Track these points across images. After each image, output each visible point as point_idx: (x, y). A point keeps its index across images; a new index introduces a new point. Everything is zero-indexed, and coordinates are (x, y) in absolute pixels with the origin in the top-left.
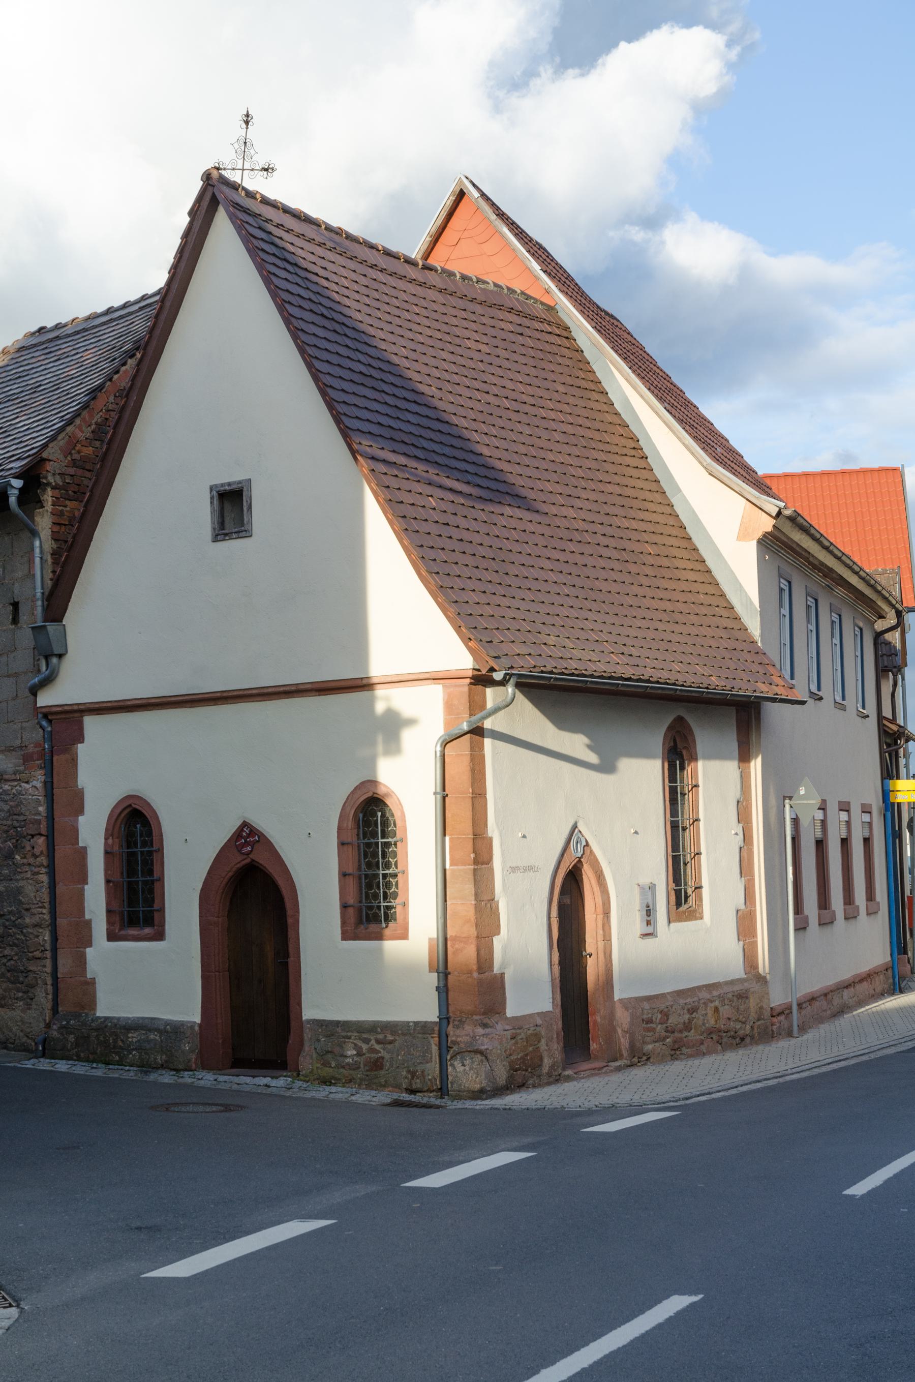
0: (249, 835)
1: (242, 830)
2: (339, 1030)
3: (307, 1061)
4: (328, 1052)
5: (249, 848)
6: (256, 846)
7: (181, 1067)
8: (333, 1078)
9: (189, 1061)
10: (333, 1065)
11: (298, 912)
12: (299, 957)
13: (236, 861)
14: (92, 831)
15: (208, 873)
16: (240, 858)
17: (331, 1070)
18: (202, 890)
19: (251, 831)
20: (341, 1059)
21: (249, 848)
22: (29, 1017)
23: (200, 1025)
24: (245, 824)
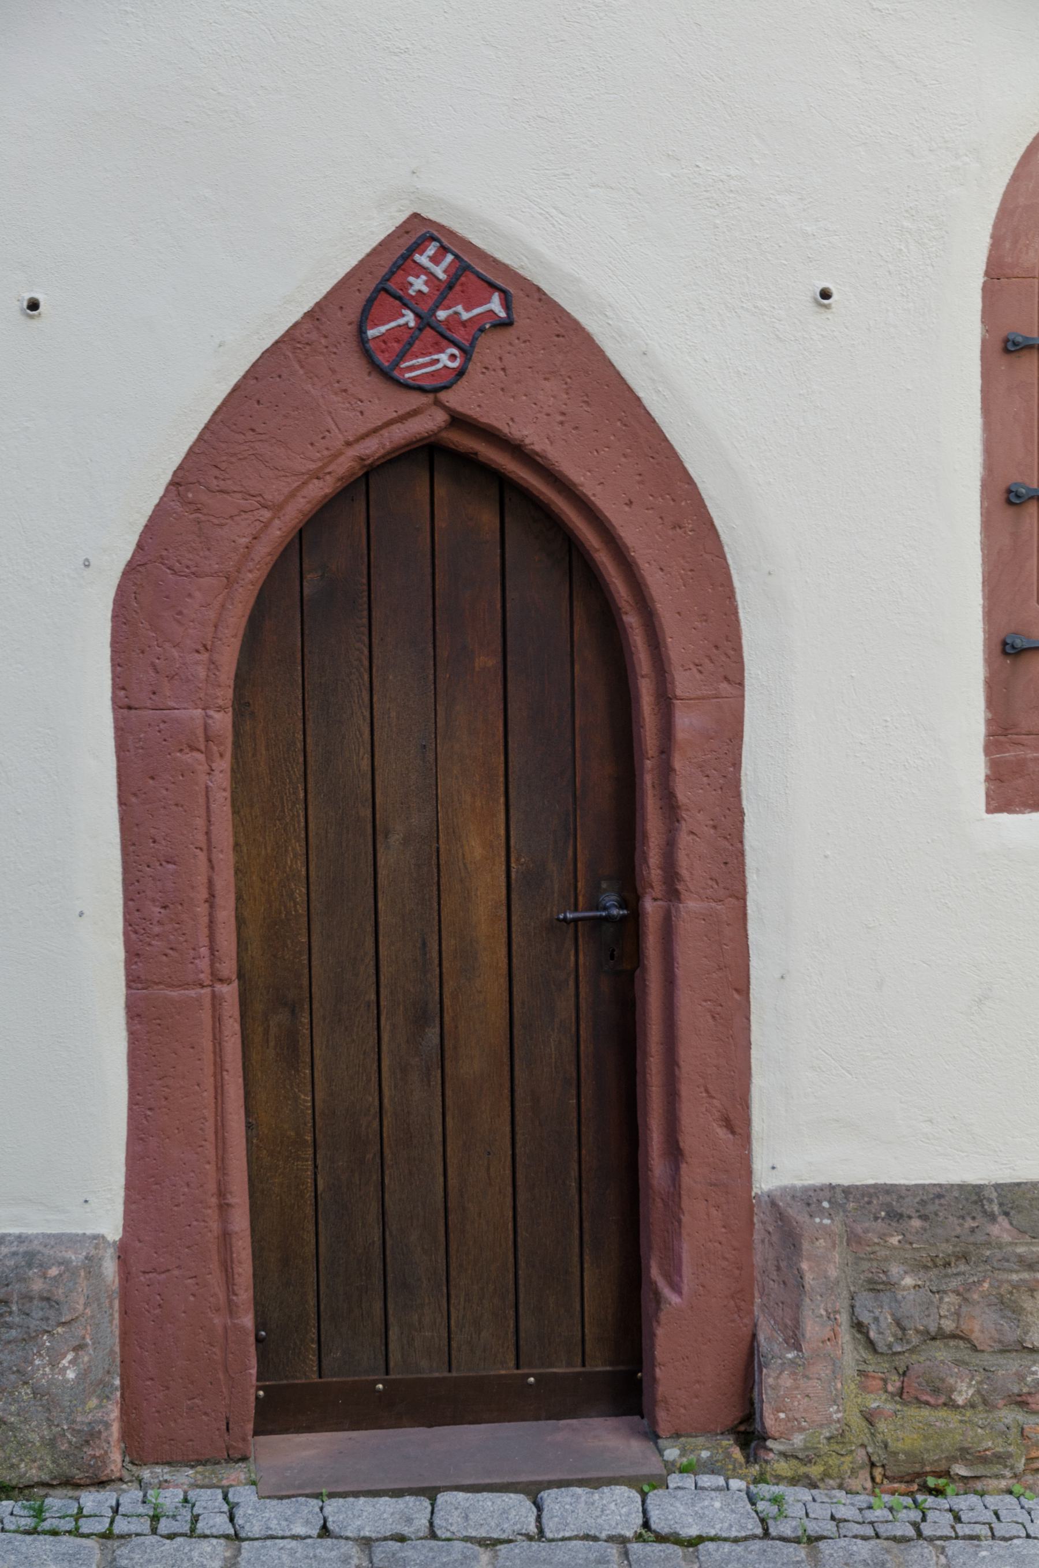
0: (446, 291)
1: (405, 263)
2: (1001, 1230)
3: (812, 1394)
4: (940, 1336)
5: (446, 359)
6: (489, 348)
7: (34, 1474)
8: (964, 1454)
9: (91, 1436)
10: (964, 1393)
11: (736, 680)
12: (739, 895)
13: (368, 421)
14: (435, 357)
15: (178, 483)
16: (382, 405)
17: (954, 1419)
18: (131, 569)
19: (461, 270)
20: (1012, 1364)
21: (446, 359)
22: (646, 1488)
23: (124, 1252)
24: (419, 234)
